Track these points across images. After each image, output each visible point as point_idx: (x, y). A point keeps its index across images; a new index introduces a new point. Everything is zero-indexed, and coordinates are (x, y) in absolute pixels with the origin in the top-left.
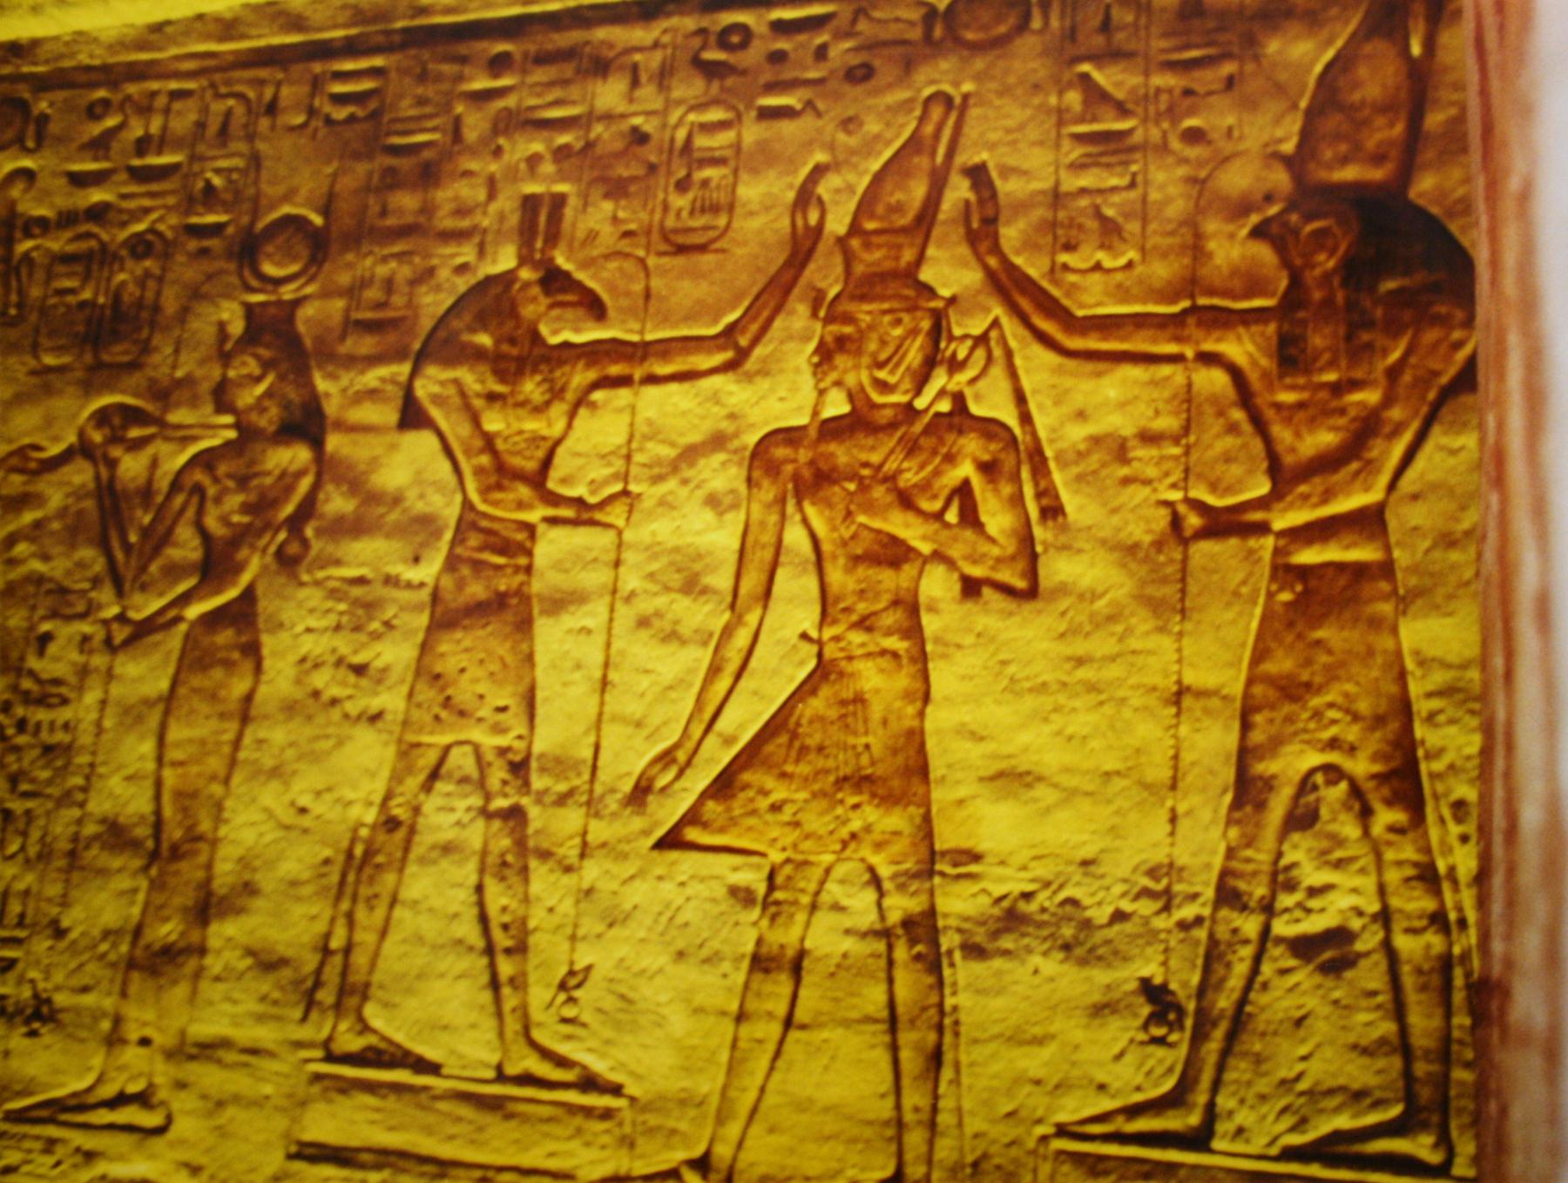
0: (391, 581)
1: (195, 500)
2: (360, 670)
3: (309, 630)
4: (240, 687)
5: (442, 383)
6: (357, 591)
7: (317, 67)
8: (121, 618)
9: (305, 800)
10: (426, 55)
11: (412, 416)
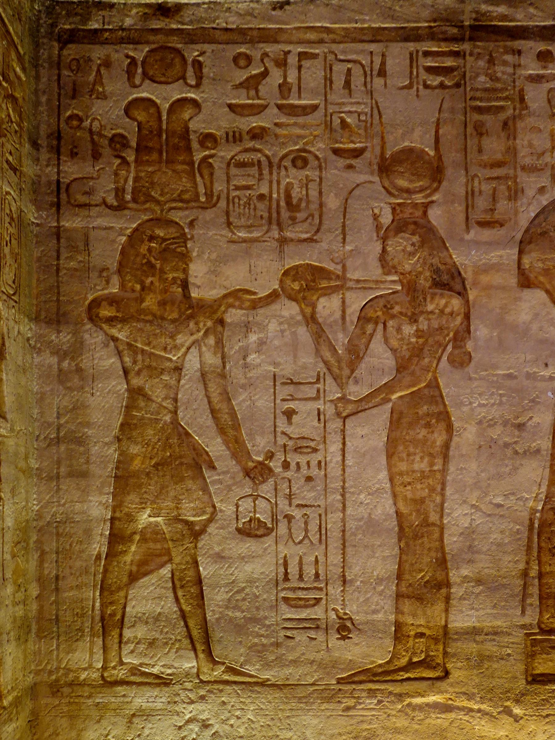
0: (528, 376)
1: (380, 327)
2: (520, 427)
3: (481, 405)
4: (439, 438)
5: (543, 261)
6: (508, 383)
7: (411, 46)
8: (343, 399)
9: (499, 500)
10: (491, 45)
11: (526, 282)
